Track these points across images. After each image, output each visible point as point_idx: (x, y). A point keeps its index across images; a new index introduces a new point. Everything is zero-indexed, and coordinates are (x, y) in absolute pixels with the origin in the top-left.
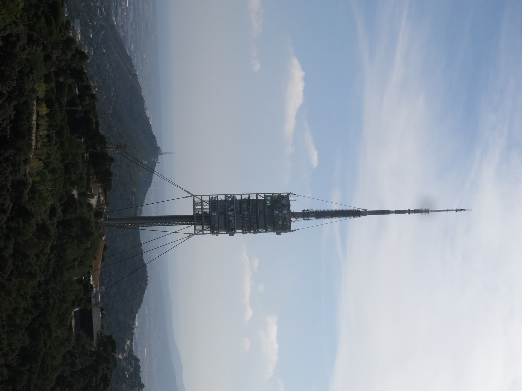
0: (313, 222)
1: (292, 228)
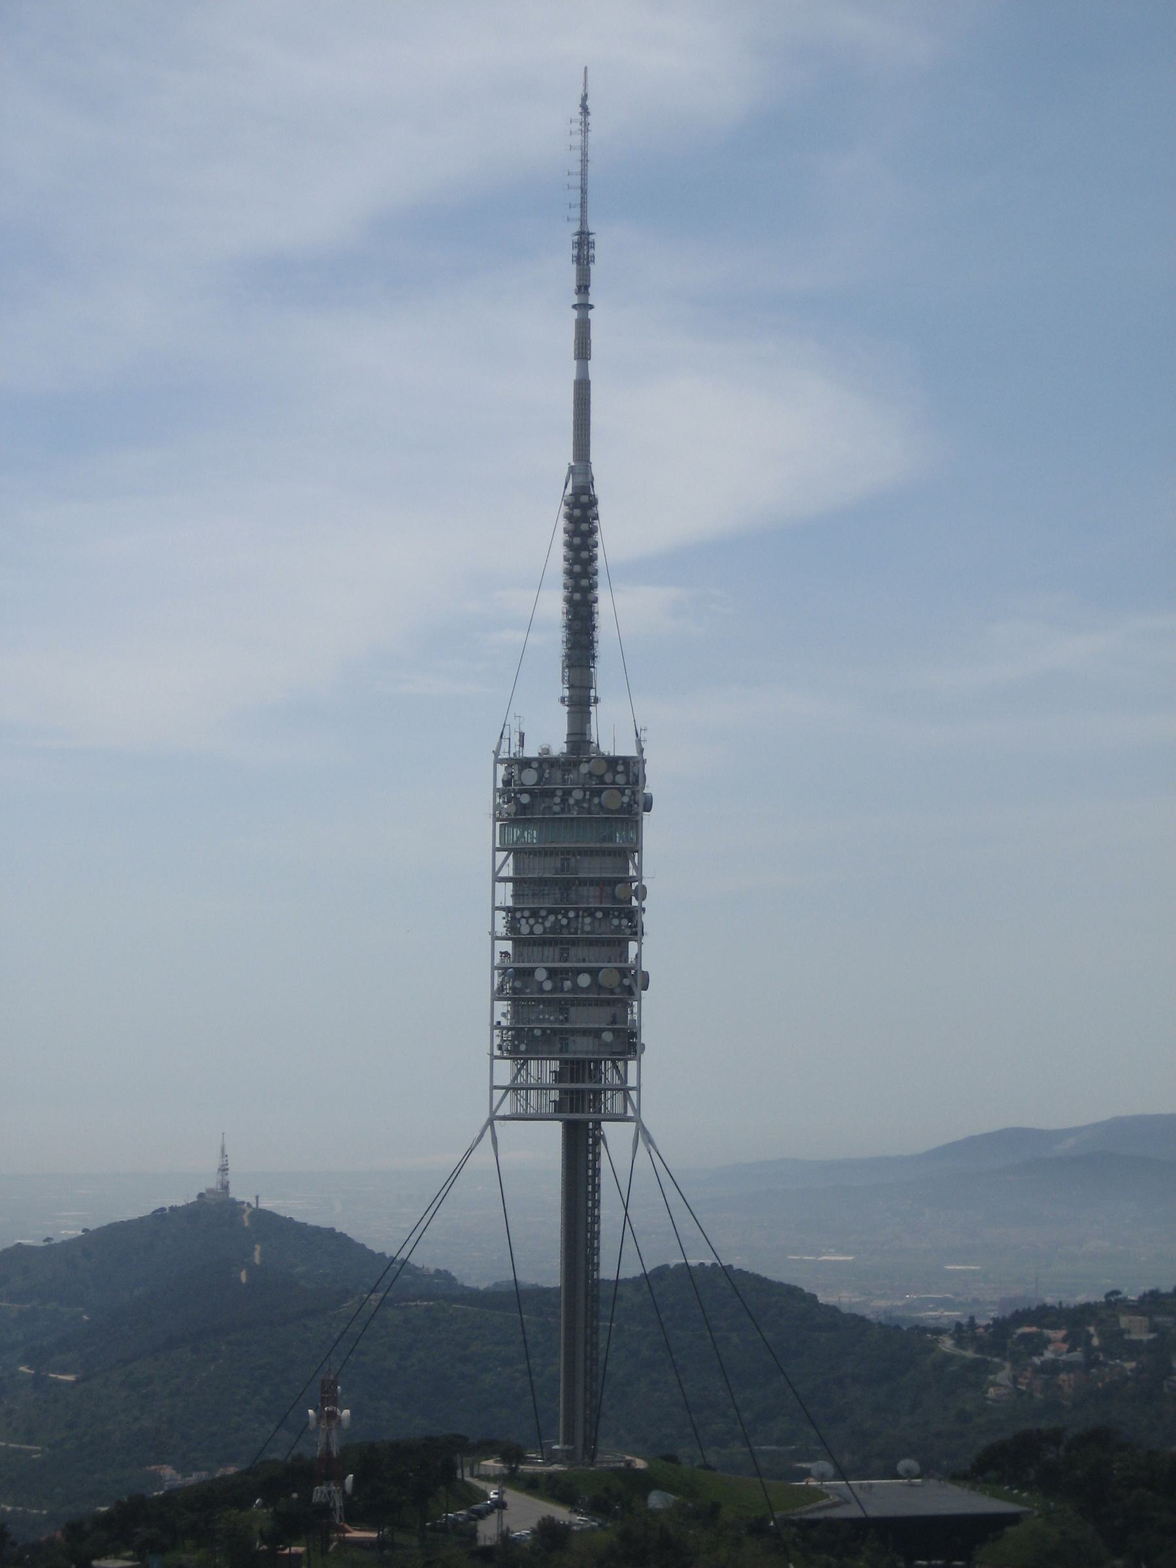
1: (631, 751)
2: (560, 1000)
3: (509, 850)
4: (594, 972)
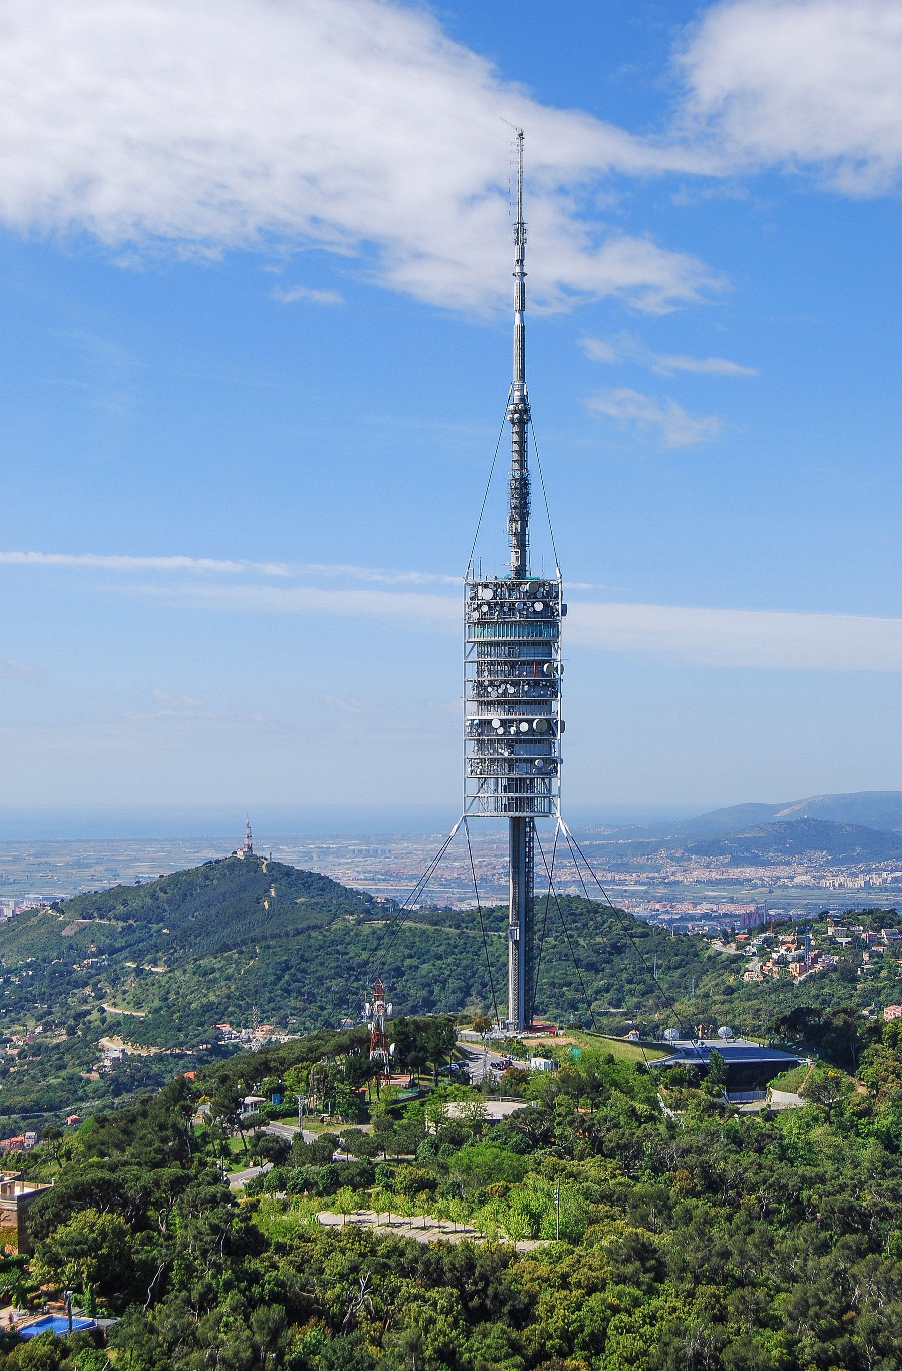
2: (508, 740)
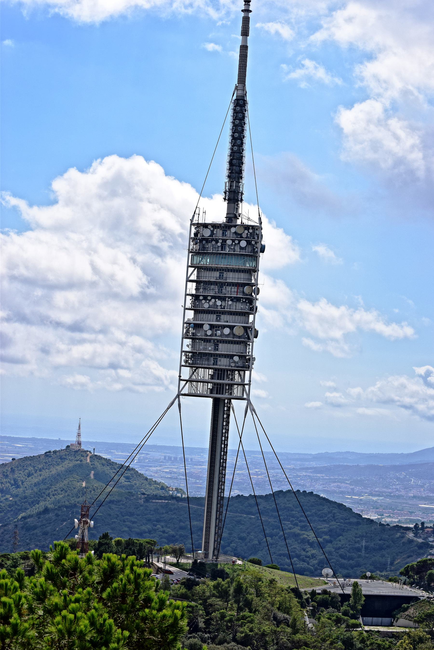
0: (247, 184)
2: (214, 340)
3: (195, 267)
4: (231, 328)
